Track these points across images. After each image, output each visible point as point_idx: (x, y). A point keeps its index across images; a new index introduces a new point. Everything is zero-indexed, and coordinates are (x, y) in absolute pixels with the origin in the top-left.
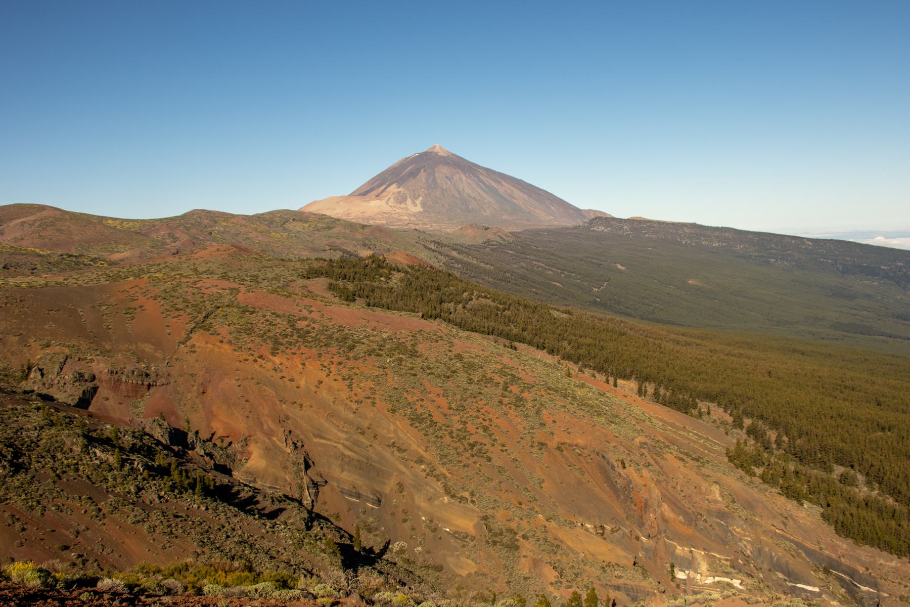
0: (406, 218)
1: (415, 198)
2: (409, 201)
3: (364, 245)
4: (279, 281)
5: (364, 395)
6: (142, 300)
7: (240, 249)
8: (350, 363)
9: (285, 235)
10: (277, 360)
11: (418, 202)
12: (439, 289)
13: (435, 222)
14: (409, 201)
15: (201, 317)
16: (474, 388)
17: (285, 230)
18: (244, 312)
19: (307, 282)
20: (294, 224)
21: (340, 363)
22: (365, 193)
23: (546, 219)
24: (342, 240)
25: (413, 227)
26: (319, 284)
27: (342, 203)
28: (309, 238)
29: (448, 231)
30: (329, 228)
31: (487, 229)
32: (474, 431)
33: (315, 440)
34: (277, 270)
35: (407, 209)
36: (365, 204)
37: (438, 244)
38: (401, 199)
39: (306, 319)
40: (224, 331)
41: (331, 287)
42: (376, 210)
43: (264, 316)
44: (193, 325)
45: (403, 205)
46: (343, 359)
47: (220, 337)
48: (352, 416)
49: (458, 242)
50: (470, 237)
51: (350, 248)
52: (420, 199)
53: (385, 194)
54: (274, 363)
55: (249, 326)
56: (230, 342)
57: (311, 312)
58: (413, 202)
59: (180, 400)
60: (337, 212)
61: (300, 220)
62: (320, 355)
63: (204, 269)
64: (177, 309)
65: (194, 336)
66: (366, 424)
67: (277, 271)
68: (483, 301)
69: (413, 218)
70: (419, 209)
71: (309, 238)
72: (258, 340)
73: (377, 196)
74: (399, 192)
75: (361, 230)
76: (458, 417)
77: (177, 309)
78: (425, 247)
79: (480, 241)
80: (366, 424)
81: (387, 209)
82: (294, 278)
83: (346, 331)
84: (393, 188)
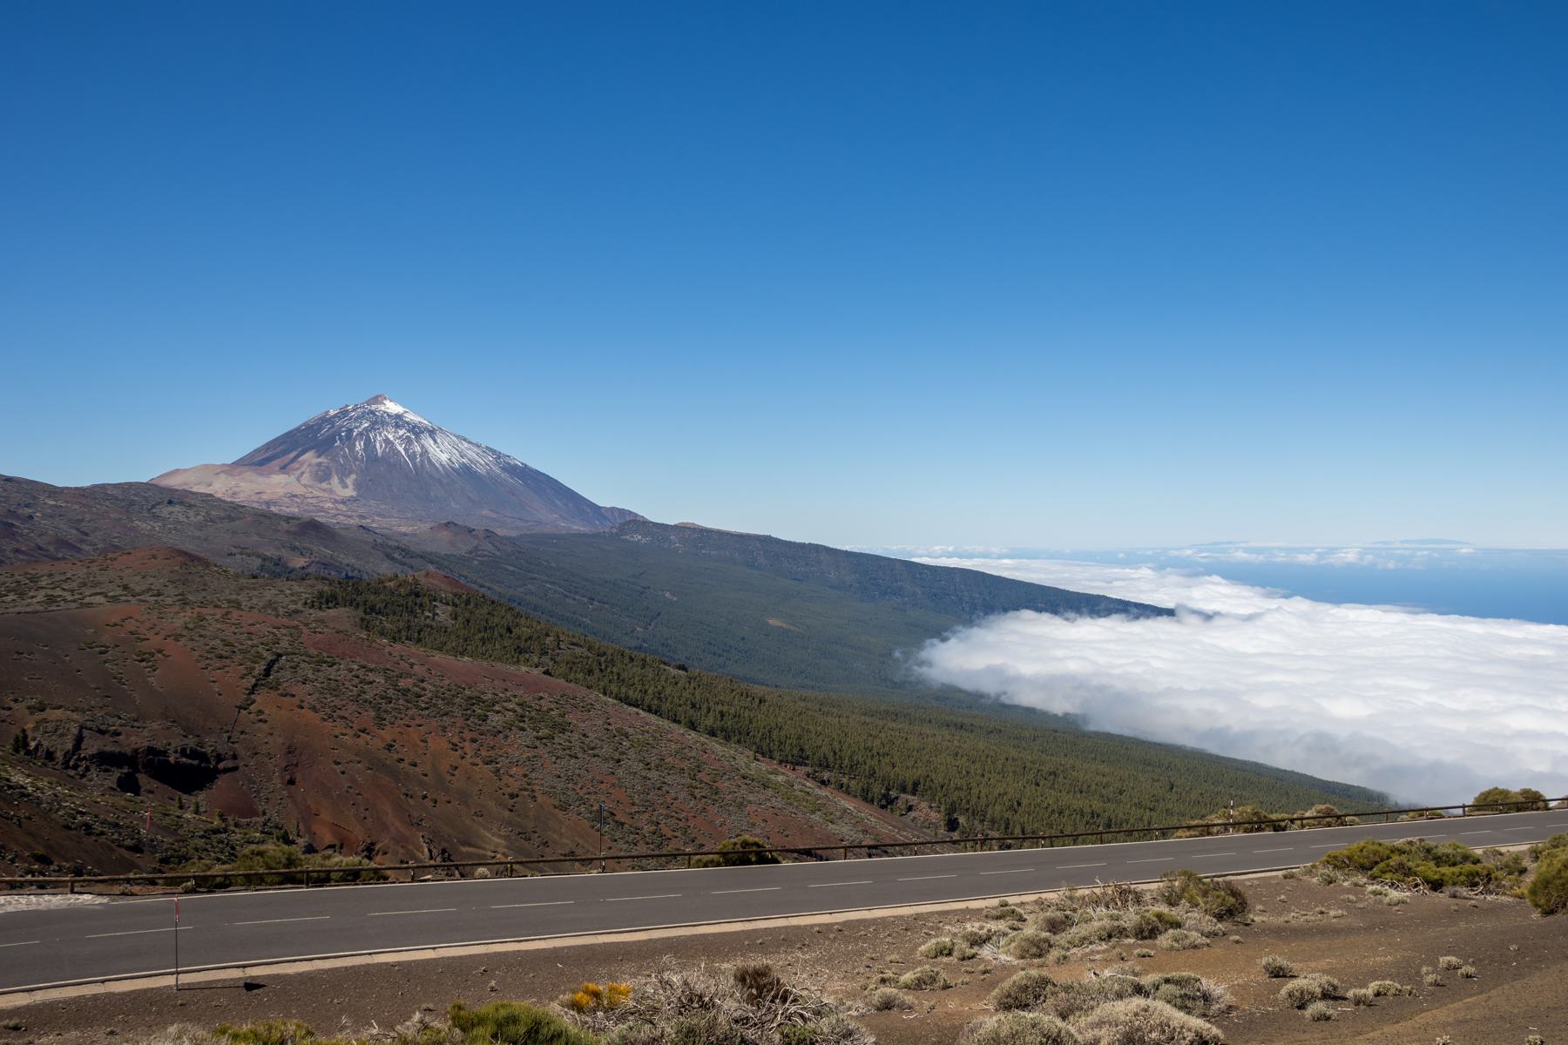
0: (329, 505)
1: (344, 474)
2: (335, 480)
3: (294, 548)
4: (275, 609)
5: (517, 784)
6: (155, 641)
7: (192, 558)
8: (490, 740)
9: (157, 525)
10: (387, 734)
11: (349, 481)
12: (509, 630)
13: (379, 515)
14: (335, 480)
15: (260, 668)
16: (653, 774)
17: (155, 517)
18: (320, 662)
19: (321, 614)
20: (171, 509)
21: (474, 741)
22: (262, 463)
23: (552, 520)
24: (256, 538)
25: (354, 521)
26: (342, 617)
27: (223, 476)
28: (198, 533)
29: (403, 529)
30: (231, 519)
31: (471, 531)
32: (669, 834)
33: (465, 849)
34: (269, 594)
35: (331, 491)
36: (260, 479)
37: (390, 549)
38: (323, 476)
39: (409, 675)
40: (300, 690)
41: (366, 625)
42: (279, 489)
43: (351, 670)
44: (253, 681)
45: (324, 485)
46: (475, 735)
47: (296, 701)
48: (507, 813)
49: (429, 550)
50: (442, 544)
51: (270, 552)
52: (353, 476)
53: (295, 465)
54: (383, 740)
55: (333, 684)
56: (314, 709)
57: (412, 665)
58: (342, 481)
59: (258, 792)
60: (220, 488)
61: (181, 503)
62: (444, 729)
63: (144, 587)
64: (221, 657)
65: (260, 697)
66: (530, 825)
67: (269, 594)
68: (578, 650)
69: (341, 506)
70: (350, 492)
71: (198, 533)
72: (353, 707)
73: (283, 469)
74: (319, 464)
75: (285, 525)
76: (646, 816)
77: (221, 657)
78: (388, 556)
79: (463, 549)
80: (530, 825)
81: (300, 490)
82: (299, 606)
83: (467, 692)
84: (309, 457)
